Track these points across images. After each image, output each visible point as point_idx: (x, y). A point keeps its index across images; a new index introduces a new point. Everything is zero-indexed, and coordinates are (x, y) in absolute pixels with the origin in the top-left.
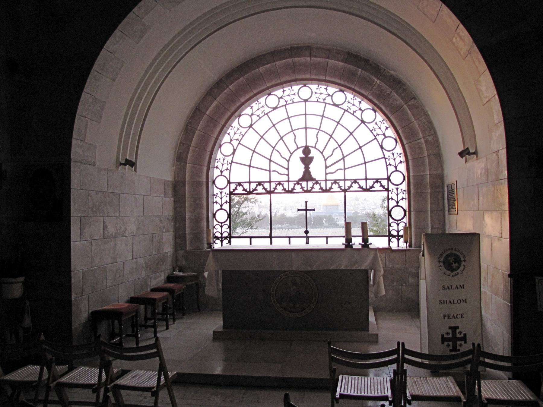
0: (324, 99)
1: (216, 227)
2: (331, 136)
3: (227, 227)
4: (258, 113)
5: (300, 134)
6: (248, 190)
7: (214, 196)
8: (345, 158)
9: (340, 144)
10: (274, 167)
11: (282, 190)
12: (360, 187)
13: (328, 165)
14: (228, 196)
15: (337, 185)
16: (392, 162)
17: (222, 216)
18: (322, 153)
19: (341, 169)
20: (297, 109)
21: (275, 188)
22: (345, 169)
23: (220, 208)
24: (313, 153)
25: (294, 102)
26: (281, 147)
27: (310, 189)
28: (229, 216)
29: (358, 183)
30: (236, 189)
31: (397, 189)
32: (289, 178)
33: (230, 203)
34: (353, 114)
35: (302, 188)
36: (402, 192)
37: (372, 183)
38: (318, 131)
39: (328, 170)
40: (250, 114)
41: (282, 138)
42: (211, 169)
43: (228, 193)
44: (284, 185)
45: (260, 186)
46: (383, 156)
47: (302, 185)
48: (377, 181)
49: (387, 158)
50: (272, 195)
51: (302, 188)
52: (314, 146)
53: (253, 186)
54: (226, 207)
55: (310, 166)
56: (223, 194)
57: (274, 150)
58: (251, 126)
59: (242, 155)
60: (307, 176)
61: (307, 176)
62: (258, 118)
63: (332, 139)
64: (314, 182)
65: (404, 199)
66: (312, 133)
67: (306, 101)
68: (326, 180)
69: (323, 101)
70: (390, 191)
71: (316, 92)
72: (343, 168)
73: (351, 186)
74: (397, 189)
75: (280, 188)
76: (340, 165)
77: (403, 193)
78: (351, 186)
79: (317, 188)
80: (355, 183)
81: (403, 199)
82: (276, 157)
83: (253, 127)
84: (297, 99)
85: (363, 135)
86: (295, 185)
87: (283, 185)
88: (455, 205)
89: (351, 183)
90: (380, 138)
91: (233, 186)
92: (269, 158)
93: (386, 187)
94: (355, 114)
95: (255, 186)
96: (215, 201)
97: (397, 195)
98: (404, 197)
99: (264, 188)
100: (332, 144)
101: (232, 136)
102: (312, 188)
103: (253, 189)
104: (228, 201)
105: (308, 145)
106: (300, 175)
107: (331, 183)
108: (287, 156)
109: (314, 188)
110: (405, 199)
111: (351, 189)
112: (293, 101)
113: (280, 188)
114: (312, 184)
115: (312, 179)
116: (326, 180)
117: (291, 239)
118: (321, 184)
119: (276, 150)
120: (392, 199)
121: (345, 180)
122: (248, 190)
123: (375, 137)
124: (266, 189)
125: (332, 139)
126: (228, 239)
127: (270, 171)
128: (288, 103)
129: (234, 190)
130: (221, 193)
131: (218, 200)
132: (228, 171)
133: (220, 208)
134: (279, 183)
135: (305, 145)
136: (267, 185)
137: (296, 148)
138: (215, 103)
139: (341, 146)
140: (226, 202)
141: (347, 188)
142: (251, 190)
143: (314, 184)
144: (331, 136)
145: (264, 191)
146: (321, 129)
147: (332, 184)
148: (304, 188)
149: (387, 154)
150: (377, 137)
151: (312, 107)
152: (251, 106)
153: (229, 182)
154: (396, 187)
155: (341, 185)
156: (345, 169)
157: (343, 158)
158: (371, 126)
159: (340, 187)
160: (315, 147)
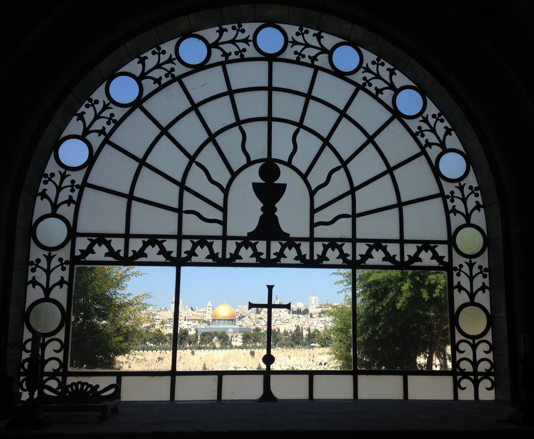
0: (314, 59)
2: (326, 142)
4: (157, 74)
6: (122, 254)
8: (357, 193)
9: (345, 158)
11: (208, 257)
14: (67, 267)
15: (337, 252)
18: (304, 177)
21: (192, 253)
27: (275, 257)
30: (90, 250)
33: (70, 284)
35: (256, 254)
38: (296, 128)
39: (318, 218)
41: (212, 138)
43: (68, 259)
44: (214, 246)
45: (153, 246)
47: (257, 246)
50: (183, 269)
51: (256, 254)
52: (286, 160)
53: (136, 245)
55: (276, 206)
57: (194, 164)
62: (157, 86)
63: (327, 149)
64: (284, 242)
68: (312, 240)
69: (309, 61)
72: (350, 214)
75: (202, 253)
79: (291, 254)
84: (251, 52)
91: (82, 244)
92: (179, 179)
99: (163, 251)
101: (88, 120)
104: (66, 279)
105: (273, 157)
106: (252, 224)
107: (324, 245)
108: (223, 177)
109: (285, 257)
112: (242, 56)
116: (312, 240)
118: (301, 248)
122: (122, 254)
129: (85, 253)
132: (73, 206)
135: (265, 156)
136: (171, 245)
137: (245, 162)
139: (349, 166)
142: (131, 254)
144: (326, 142)
145: (162, 259)
146: (305, 123)
148: (262, 254)
152: (142, 56)
155: (345, 252)
156: (354, 216)
157: (353, 191)
159: (343, 255)
160: (289, 164)
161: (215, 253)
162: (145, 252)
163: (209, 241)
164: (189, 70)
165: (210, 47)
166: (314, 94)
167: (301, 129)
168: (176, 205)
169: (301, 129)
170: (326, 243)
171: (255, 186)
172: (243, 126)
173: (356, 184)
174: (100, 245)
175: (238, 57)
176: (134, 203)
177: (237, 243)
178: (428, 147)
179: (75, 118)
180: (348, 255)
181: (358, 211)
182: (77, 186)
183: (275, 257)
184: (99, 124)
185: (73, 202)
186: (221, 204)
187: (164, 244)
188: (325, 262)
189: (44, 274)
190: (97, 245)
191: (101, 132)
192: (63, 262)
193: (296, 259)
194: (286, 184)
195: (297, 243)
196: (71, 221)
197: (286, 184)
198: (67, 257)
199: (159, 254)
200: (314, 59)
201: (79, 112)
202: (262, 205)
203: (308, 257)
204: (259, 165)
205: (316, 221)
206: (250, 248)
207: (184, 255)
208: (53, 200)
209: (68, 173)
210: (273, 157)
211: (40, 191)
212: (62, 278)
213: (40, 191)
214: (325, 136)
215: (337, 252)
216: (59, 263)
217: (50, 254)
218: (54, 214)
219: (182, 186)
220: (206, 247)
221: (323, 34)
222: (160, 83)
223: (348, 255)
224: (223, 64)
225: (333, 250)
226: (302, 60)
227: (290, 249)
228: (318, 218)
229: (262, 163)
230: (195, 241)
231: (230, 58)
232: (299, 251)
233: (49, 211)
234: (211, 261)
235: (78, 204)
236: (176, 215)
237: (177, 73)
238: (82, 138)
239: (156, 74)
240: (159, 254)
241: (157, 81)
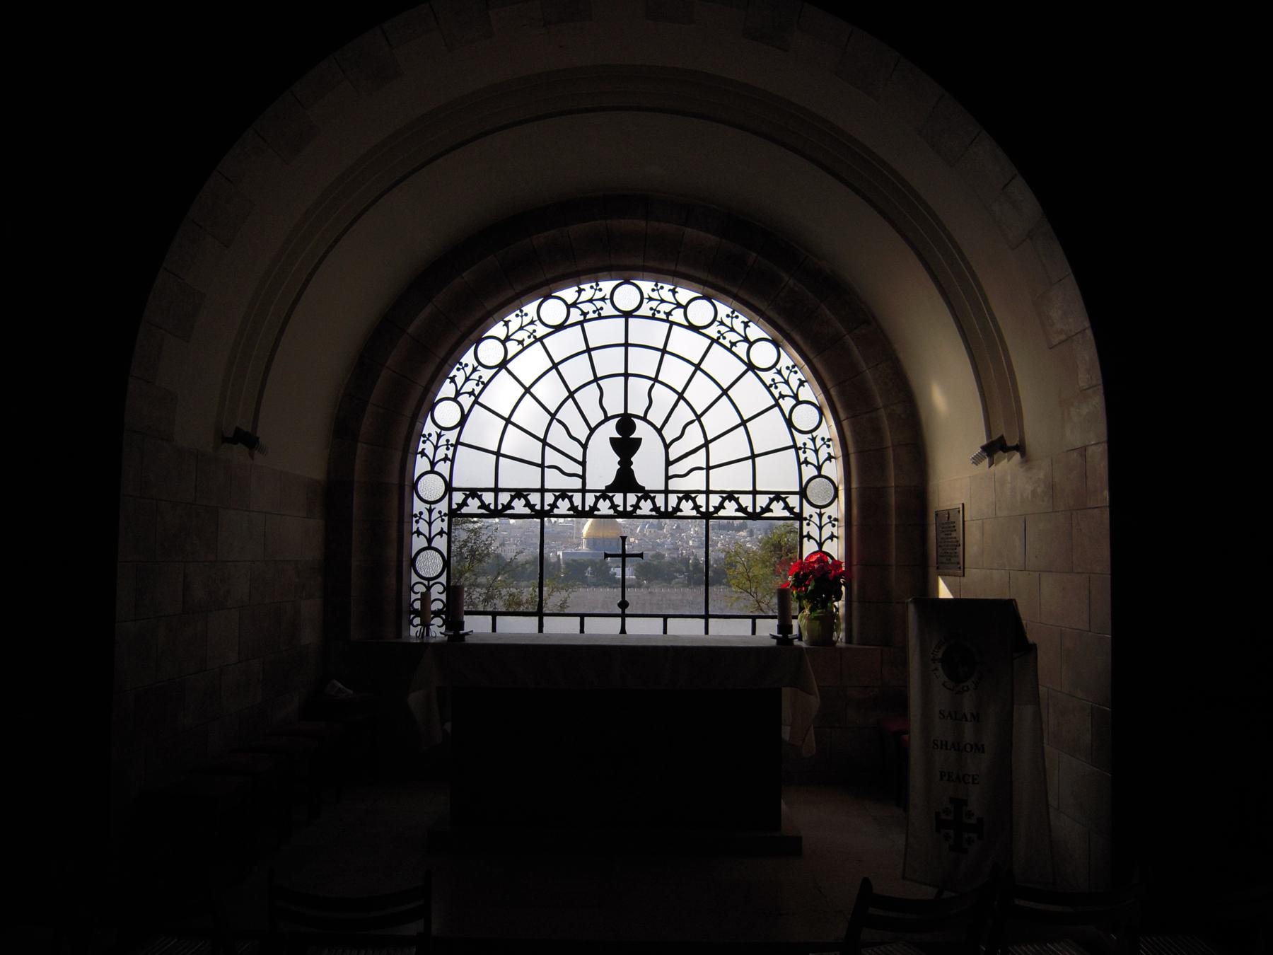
0: (668, 314)
1: (417, 588)
2: (681, 396)
3: (441, 588)
4: (520, 336)
5: (613, 388)
6: (492, 507)
7: (414, 519)
8: (710, 445)
9: (699, 413)
10: (552, 457)
11: (569, 510)
12: (741, 508)
13: (672, 458)
14: (446, 518)
15: (690, 504)
16: (811, 456)
17: (430, 564)
18: (659, 431)
19: (701, 469)
20: (606, 331)
21: (554, 506)
22: (708, 468)
23: (426, 545)
24: (641, 430)
25: (602, 315)
26: (569, 414)
28: (447, 564)
29: (737, 500)
30: (464, 503)
31: (820, 515)
32: (584, 484)
33: (449, 534)
34: (730, 350)
35: (614, 506)
36: (830, 522)
37: (768, 501)
39: (673, 470)
40: (503, 339)
41: (571, 395)
42: (410, 457)
44: (574, 499)
45: (519, 499)
46: (792, 444)
47: (614, 499)
48: (778, 496)
49: (800, 448)
51: (614, 506)
52: (642, 415)
53: (504, 498)
54: (441, 543)
55: (632, 459)
56: (435, 515)
57: (555, 421)
58: (503, 365)
59: (483, 429)
60: (625, 481)
61: (625, 481)
62: (520, 347)
63: (682, 402)
64: (640, 495)
65: (835, 539)
66: (639, 388)
67: (627, 315)
68: (667, 492)
69: (664, 317)
70: (806, 519)
71: (651, 296)
72: (705, 467)
73: (721, 506)
74: (820, 515)
75: (563, 506)
76: (699, 459)
77: (834, 526)
78: (721, 506)
79: (646, 507)
80: (730, 501)
81: (832, 537)
82: (557, 436)
83: (508, 366)
85: (751, 395)
86: (597, 499)
87: (570, 499)
88: (958, 556)
89: (721, 499)
90: (787, 404)
91: (458, 497)
92: (542, 437)
93: (797, 510)
94: (734, 349)
95: (509, 498)
96: (415, 529)
97: (821, 528)
98: (836, 534)
99: (528, 504)
100: (683, 413)
102: (637, 507)
103: (503, 504)
104: (446, 530)
106: (610, 478)
107: (678, 497)
108: (582, 433)
109: (641, 509)
110: (837, 538)
111: (722, 513)
112: (599, 314)
113: (563, 506)
114: (636, 499)
115: (636, 488)
116: (667, 492)
117: (586, 619)
118: (656, 500)
119: (559, 421)
120: (809, 537)
121: (708, 492)
122: (492, 507)
123: (776, 400)
124: (531, 507)
125: (682, 402)
126: (444, 616)
127: (542, 466)
128: (588, 317)
129: (460, 506)
130: (430, 511)
131: (423, 527)
132: (449, 463)
133: (426, 545)
134: (563, 494)
135: (622, 411)
136: (535, 498)
138: (427, 311)
139: (702, 419)
140: (441, 533)
141: (711, 509)
142: (500, 507)
143: (639, 499)
144: (681, 396)
145: (527, 511)
146: (659, 379)
147: (680, 500)
149: (801, 439)
150: (781, 401)
151: (643, 331)
152: (506, 319)
153: (449, 489)
154: (818, 511)
156: (708, 468)
157: (706, 444)
158: (768, 377)
159: (696, 507)
160: (644, 419)
161: (575, 505)
162: (512, 504)
163: (570, 494)
164: (551, 330)
165: (569, 307)
166: (668, 349)
167: (656, 384)
168: (540, 462)
169: (656, 384)
170: (681, 495)
171: (613, 441)
172: (599, 382)
173: (709, 439)
174: (473, 499)
175: (596, 315)
176: (501, 458)
177: (596, 496)
178: (781, 399)
179: (448, 381)
180: (701, 507)
181: (711, 465)
182: (452, 445)
183: (632, 509)
184: (469, 386)
185: (449, 459)
186: (581, 460)
187: (529, 497)
188: (679, 514)
189: (427, 525)
190: (470, 498)
191: (471, 393)
192: (442, 514)
193: (651, 510)
194: (641, 439)
195: (652, 495)
196: (448, 480)
197: (641, 439)
198: (445, 510)
199: (525, 506)
200: (668, 314)
201: (451, 375)
202: (619, 459)
203: (663, 509)
204: (617, 420)
205: (670, 475)
206: (607, 500)
207: (546, 508)
208: (431, 459)
209: (443, 432)
210: (629, 412)
211: (420, 450)
212: (442, 529)
213: (420, 450)
214: (680, 391)
215: (690, 504)
216: (439, 515)
217: (430, 507)
218: (432, 471)
219: (544, 443)
220: (566, 500)
221: (677, 289)
222: (523, 345)
223: (701, 507)
224: (581, 323)
225: (687, 501)
226: (657, 316)
227: (646, 501)
228: (671, 472)
229: (617, 419)
230: (557, 494)
231: (588, 317)
232: (654, 503)
233: (429, 469)
234: (571, 512)
235: (452, 461)
236: (540, 469)
237: (538, 335)
238: (455, 400)
239: (520, 336)
240: (525, 506)
241: (521, 342)
